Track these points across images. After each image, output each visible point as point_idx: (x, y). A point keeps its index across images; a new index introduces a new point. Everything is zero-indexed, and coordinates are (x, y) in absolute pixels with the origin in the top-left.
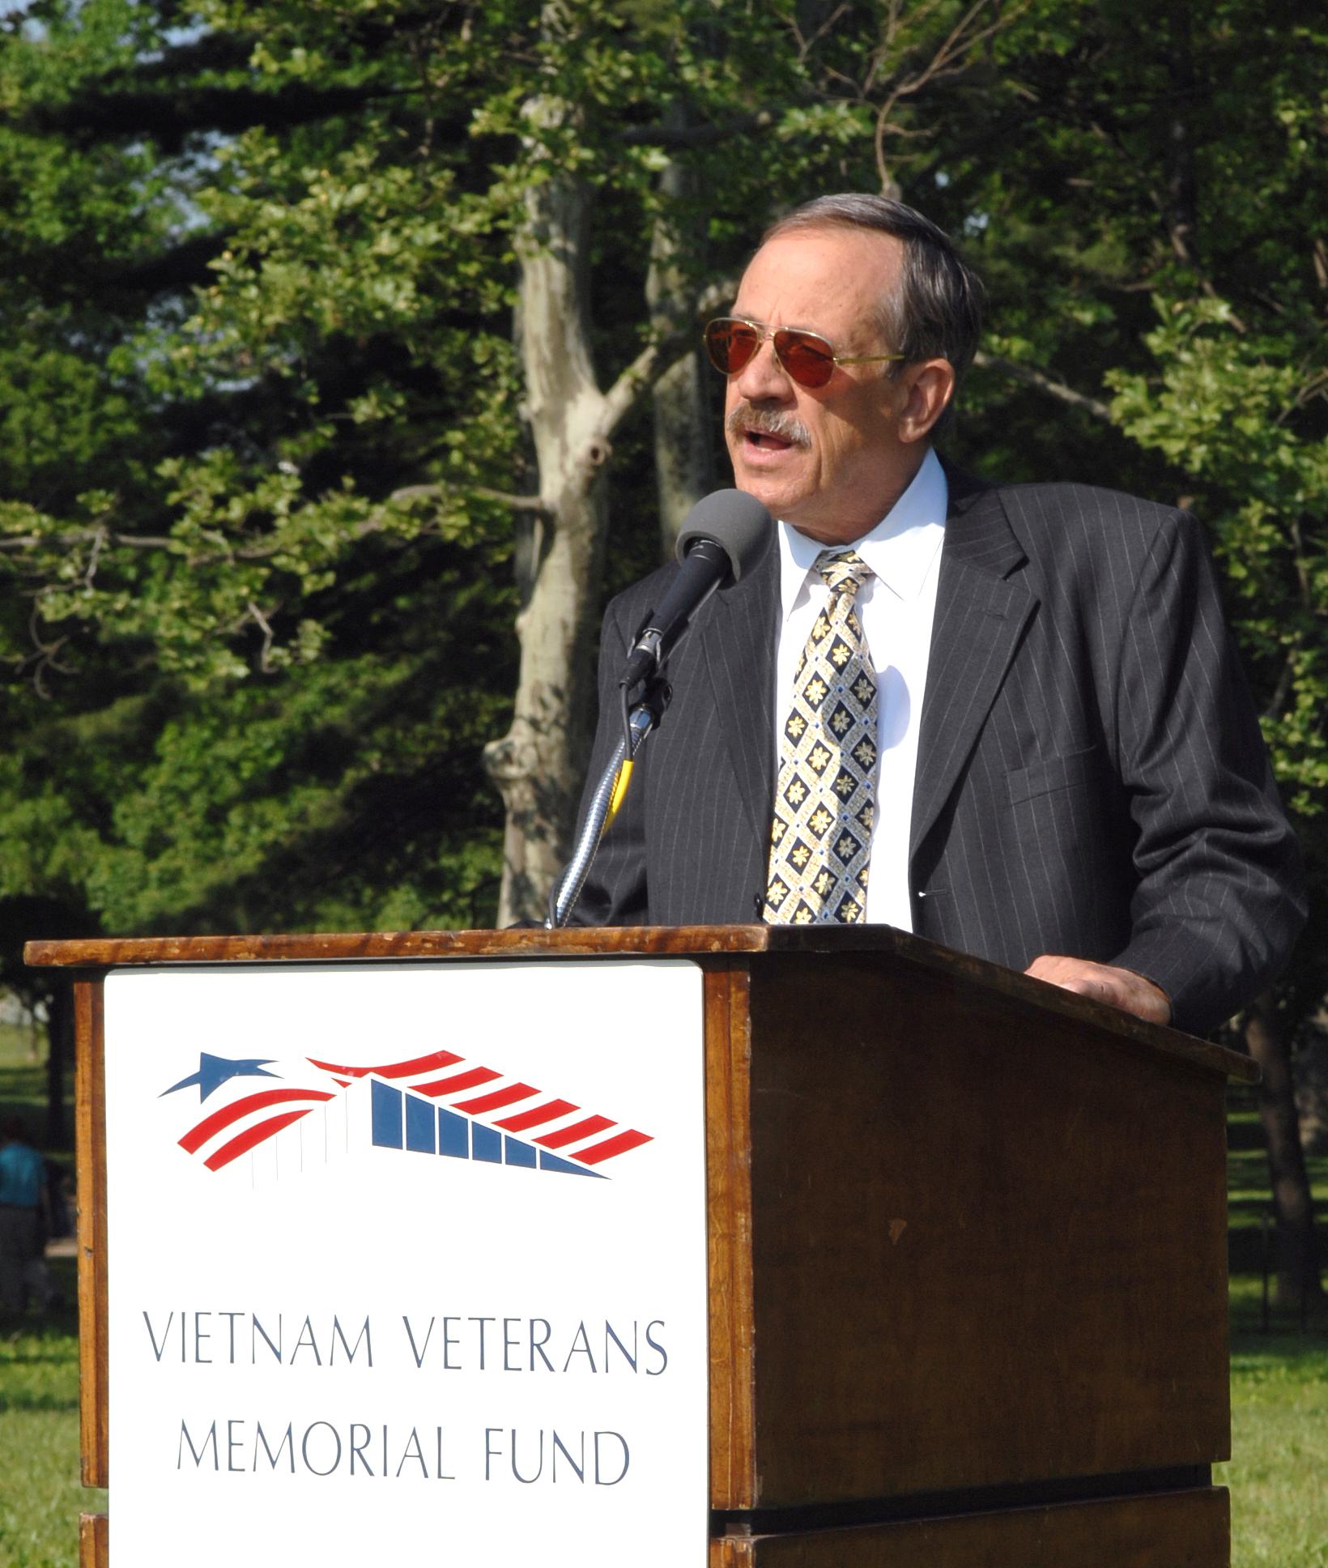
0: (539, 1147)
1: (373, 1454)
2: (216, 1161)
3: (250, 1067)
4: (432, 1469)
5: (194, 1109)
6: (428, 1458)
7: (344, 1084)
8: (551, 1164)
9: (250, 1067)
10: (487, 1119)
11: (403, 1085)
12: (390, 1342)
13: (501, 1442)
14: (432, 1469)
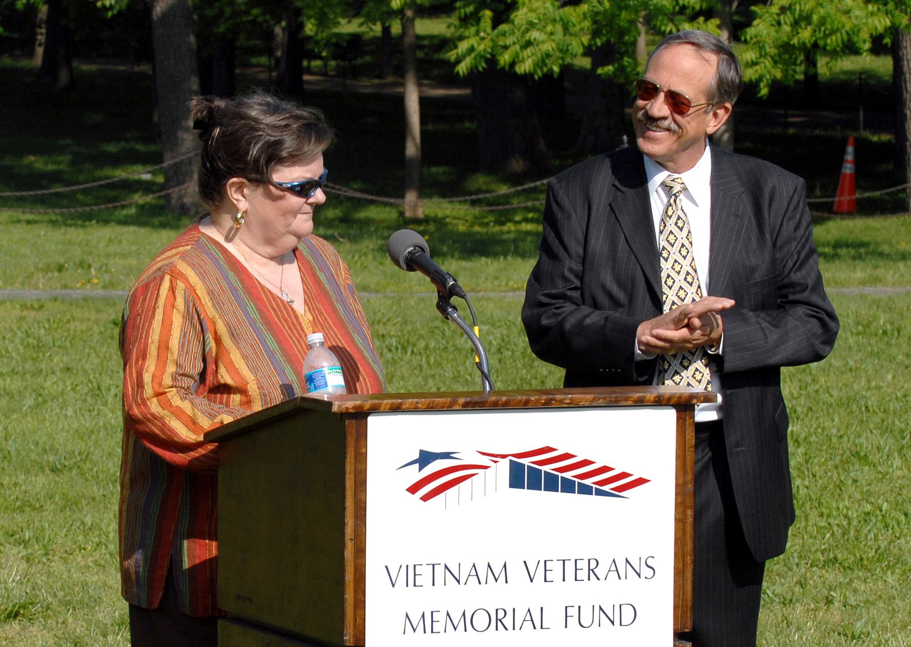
0: (594, 486)
1: (508, 621)
2: (425, 498)
3: (446, 456)
4: (538, 625)
5: (415, 474)
6: (536, 620)
7: (496, 462)
8: (600, 493)
9: (446, 456)
10: (568, 475)
11: (526, 461)
12: (517, 572)
13: (573, 612)
14: (538, 625)
